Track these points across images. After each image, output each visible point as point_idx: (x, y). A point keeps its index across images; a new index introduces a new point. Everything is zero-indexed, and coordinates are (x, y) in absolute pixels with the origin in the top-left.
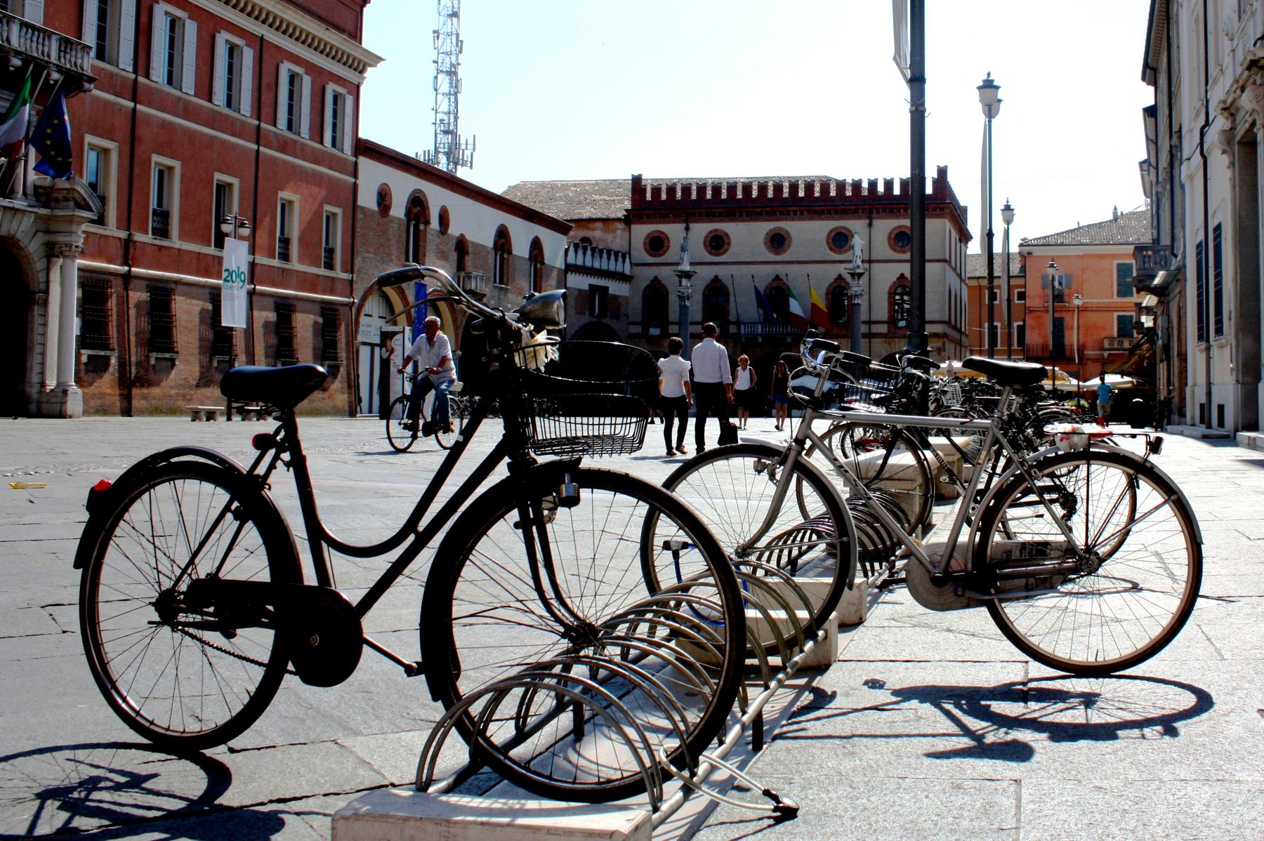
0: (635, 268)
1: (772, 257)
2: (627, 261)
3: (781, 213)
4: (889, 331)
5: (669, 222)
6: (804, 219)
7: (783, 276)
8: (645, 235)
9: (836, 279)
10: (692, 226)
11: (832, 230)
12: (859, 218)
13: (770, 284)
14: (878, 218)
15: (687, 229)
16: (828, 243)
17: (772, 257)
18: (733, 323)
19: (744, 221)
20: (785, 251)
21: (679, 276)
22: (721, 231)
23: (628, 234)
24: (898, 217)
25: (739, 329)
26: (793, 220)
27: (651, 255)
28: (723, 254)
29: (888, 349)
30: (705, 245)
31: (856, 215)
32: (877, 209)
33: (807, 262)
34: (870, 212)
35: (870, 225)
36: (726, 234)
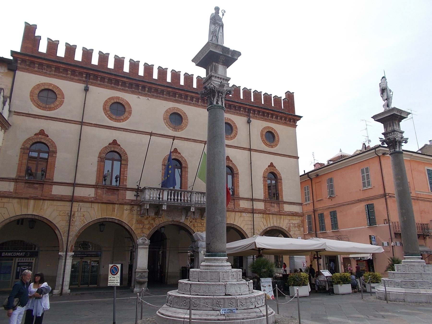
0: (15, 117)
1: (171, 133)
3: (180, 96)
4: (266, 208)
6: (198, 106)
10: (91, 88)
12: (241, 115)
14: (253, 118)
15: (86, 90)
17: (171, 133)
18: (132, 189)
19: (145, 95)
20: (182, 129)
22: (123, 100)
23: (10, 80)
24: (266, 120)
26: (189, 104)
28: (124, 120)
29: (265, 224)
30: (104, 109)
32: (254, 111)
34: (249, 112)
35: (249, 122)
36: (128, 104)
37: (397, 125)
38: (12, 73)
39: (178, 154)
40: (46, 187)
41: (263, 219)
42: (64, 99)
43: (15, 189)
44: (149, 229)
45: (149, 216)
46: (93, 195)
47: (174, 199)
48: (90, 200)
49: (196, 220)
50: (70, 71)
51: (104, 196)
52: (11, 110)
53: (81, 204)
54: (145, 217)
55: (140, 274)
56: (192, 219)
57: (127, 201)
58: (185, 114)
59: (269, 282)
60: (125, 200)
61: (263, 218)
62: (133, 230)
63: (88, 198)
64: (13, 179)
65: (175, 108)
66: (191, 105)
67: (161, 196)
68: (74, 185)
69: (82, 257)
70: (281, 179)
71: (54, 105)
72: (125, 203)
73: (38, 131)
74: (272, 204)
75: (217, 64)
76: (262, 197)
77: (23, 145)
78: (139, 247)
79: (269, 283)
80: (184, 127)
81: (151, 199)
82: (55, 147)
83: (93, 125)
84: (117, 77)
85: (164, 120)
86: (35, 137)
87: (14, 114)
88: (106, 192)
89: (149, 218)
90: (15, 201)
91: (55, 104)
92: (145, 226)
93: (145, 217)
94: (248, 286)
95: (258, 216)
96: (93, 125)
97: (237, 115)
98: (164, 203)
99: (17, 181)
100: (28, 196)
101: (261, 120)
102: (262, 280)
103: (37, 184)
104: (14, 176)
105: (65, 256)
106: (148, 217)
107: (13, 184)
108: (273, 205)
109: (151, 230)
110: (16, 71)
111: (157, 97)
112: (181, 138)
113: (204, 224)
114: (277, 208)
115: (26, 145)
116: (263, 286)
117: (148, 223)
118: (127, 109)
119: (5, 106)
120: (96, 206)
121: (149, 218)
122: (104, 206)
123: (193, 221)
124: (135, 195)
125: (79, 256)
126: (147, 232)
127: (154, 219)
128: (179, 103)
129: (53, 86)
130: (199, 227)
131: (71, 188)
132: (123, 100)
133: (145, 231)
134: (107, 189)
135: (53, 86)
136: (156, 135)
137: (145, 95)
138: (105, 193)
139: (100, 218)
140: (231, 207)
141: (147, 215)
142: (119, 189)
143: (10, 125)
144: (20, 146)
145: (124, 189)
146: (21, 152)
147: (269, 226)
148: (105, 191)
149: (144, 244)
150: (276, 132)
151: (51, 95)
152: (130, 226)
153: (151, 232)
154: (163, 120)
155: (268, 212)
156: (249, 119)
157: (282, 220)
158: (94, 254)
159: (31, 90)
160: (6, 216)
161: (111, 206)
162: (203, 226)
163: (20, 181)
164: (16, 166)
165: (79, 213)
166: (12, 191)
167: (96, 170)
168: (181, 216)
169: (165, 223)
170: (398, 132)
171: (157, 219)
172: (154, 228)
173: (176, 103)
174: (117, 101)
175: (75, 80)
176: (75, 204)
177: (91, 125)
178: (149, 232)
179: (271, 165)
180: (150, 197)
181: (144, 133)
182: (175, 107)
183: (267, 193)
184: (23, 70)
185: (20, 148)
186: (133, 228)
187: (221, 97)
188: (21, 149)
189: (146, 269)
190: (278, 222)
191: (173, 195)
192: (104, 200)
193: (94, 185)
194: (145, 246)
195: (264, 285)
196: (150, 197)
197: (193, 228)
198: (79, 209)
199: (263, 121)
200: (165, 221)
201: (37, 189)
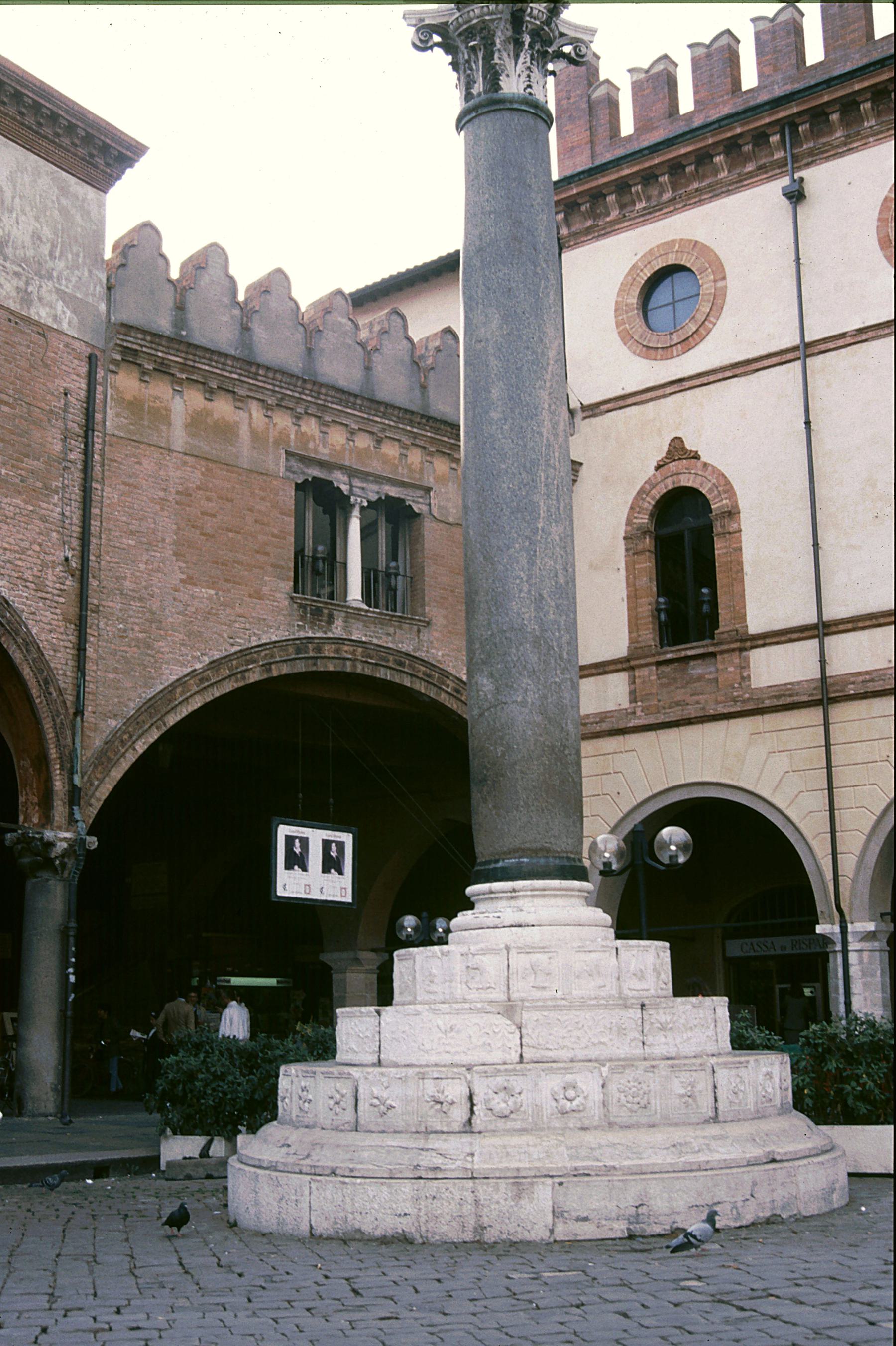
5: (717, 191)
27: (649, 352)
40: (728, 666)
42: (724, 278)
50: (719, 154)
77: (629, 522)
82: (729, 490)
83: (849, 340)
87: (585, 418)
96: (849, 340)
99: (633, 663)
104: (619, 647)
129: (677, 246)
135: (677, 246)
143: (581, 464)
146: (627, 550)
151: (680, 284)
177: (841, 342)
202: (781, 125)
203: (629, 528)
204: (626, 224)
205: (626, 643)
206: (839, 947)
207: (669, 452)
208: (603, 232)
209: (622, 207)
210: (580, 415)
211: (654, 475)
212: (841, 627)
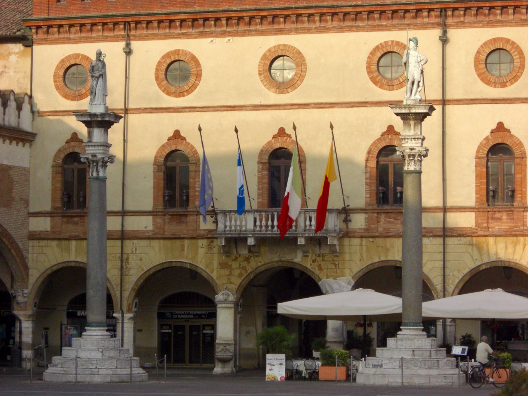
2: (26, 107)
4: (477, 224)
6: (326, 30)
7: (289, 131)
8: (56, 62)
9: (383, 134)
10: (135, 45)
11: (377, 48)
12: (424, 26)
13: (269, 143)
16: (369, 72)
17: (274, 98)
19: (223, 34)
21: (88, 124)
22: (185, 53)
24: (490, 24)
25: (216, 222)
26: (308, 31)
27: (66, 96)
28: (189, 91)
30: (157, 78)
31: (419, 21)
33: (332, 105)
36: (194, 59)
37: (412, 126)
38: (29, 49)
39: (285, 138)
41: (470, 247)
43: (52, 227)
44: (240, 275)
45: (240, 255)
46: (150, 227)
47: (267, 226)
48: (147, 235)
49: (323, 256)
51: (167, 227)
52: (34, 109)
53: (135, 241)
54: (233, 257)
55: (222, 347)
56: (316, 255)
57: (202, 232)
58: (299, 53)
59: (281, 359)
60: (198, 232)
61: (472, 245)
62: (215, 278)
63: (144, 232)
64: (47, 213)
65: (279, 46)
66: (312, 33)
67: (244, 223)
68: (123, 213)
69: (187, 318)
70: (523, 155)
71: (85, 89)
72: (198, 236)
73: (69, 137)
74: (494, 214)
75: (91, 129)
76: (472, 202)
77: (54, 161)
78: (219, 306)
79: (280, 361)
80: (299, 82)
81: (228, 228)
84: (169, 16)
85: (260, 74)
86: (67, 146)
88: (169, 220)
89: (239, 258)
90: (54, 243)
91: (87, 87)
92: (232, 272)
93: (233, 257)
94: (102, 352)
95: (459, 242)
97: (415, 29)
98: (248, 234)
99: (53, 215)
100: (67, 235)
101: (477, 27)
102: (268, 356)
103: (77, 216)
104: (48, 208)
105: (121, 319)
106: (238, 256)
107: (48, 219)
108: (497, 215)
109: (243, 278)
110: (32, 45)
111: (244, 33)
112: (292, 105)
113: (339, 264)
114: (509, 221)
115: (57, 160)
116: (270, 364)
117: (238, 265)
118: (194, 70)
119: (21, 113)
120: (156, 243)
121: (239, 258)
122: (168, 242)
123: (318, 259)
124: (214, 222)
125: (182, 316)
126: (237, 281)
127: (247, 259)
128: (288, 34)
129: (80, 57)
130: (329, 270)
131: (119, 219)
132: (186, 54)
133: (233, 279)
134: (171, 215)
135: (80, 57)
136: (244, 108)
137: (222, 34)
138: (168, 222)
139: (164, 262)
140: (396, 228)
141: (235, 253)
142: (187, 213)
144: (50, 163)
145: (195, 213)
146: (53, 171)
147: (486, 260)
148: (168, 219)
149: (225, 301)
150: (518, 46)
152: (210, 273)
153: (244, 282)
154: (258, 75)
155: (482, 233)
156: (445, 32)
157: (519, 248)
158: (204, 314)
159: (55, 72)
160: (48, 265)
161: (178, 242)
162: (337, 267)
163: (55, 215)
164: (50, 193)
165: (134, 257)
166: (49, 229)
167: (152, 187)
168: (296, 252)
169: (266, 266)
170: (408, 139)
171: (252, 258)
172: (247, 274)
173: (282, 34)
174: (175, 58)
175: (110, 39)
176: (128, 243)
177: (138, 111)
178: (241, 281)
179: (500, 127)
180: (226, 227)
181: (224, 109)
182: (280, 45)
183: (484, 193)
184: (42, 42)
185: (51, 165)
186: (214, 275)
187: (95, 167)
188: (52, 167)
189: (231, 340)
190: (510, 250)
191: (264, 219)
192: (168, 234)
193: (150, 212)
194: (228, 305)
195: (272, 363)
196: (226, 227)
197: (317, 272)
198: (134, 250)
199: (482, 27)
200: (267, 261)
201: (78, 224)
202: (125, 23)
203: (54, 163)
204: (61, 41)
205: (50, 207)
206: (121, 321)
207: (71, 138)
208: (51, 42)
209: (59, 32)
210: (36, 114)
211: (65, 145)
212: (129, 214)
